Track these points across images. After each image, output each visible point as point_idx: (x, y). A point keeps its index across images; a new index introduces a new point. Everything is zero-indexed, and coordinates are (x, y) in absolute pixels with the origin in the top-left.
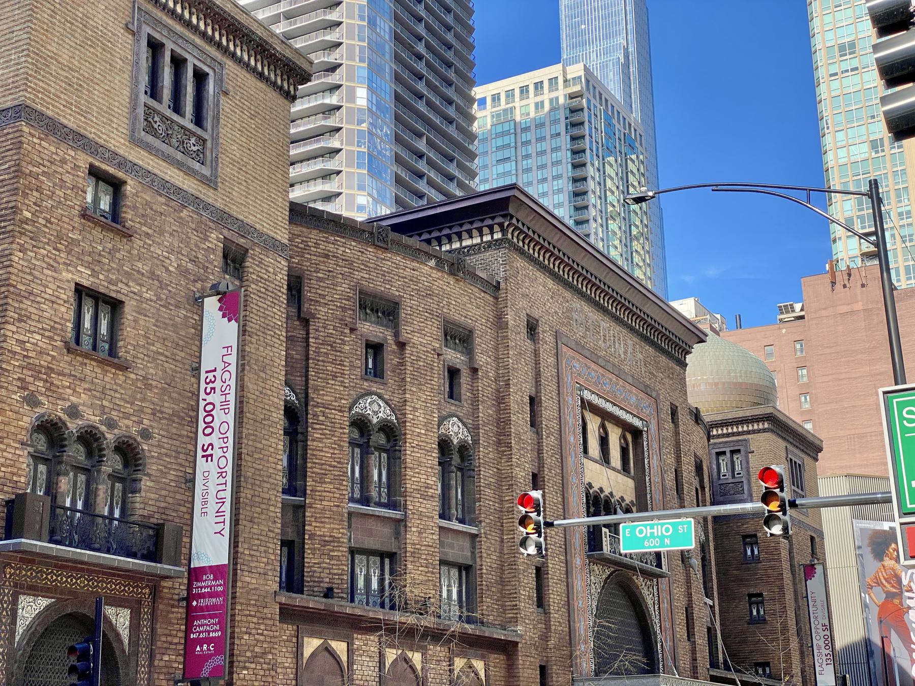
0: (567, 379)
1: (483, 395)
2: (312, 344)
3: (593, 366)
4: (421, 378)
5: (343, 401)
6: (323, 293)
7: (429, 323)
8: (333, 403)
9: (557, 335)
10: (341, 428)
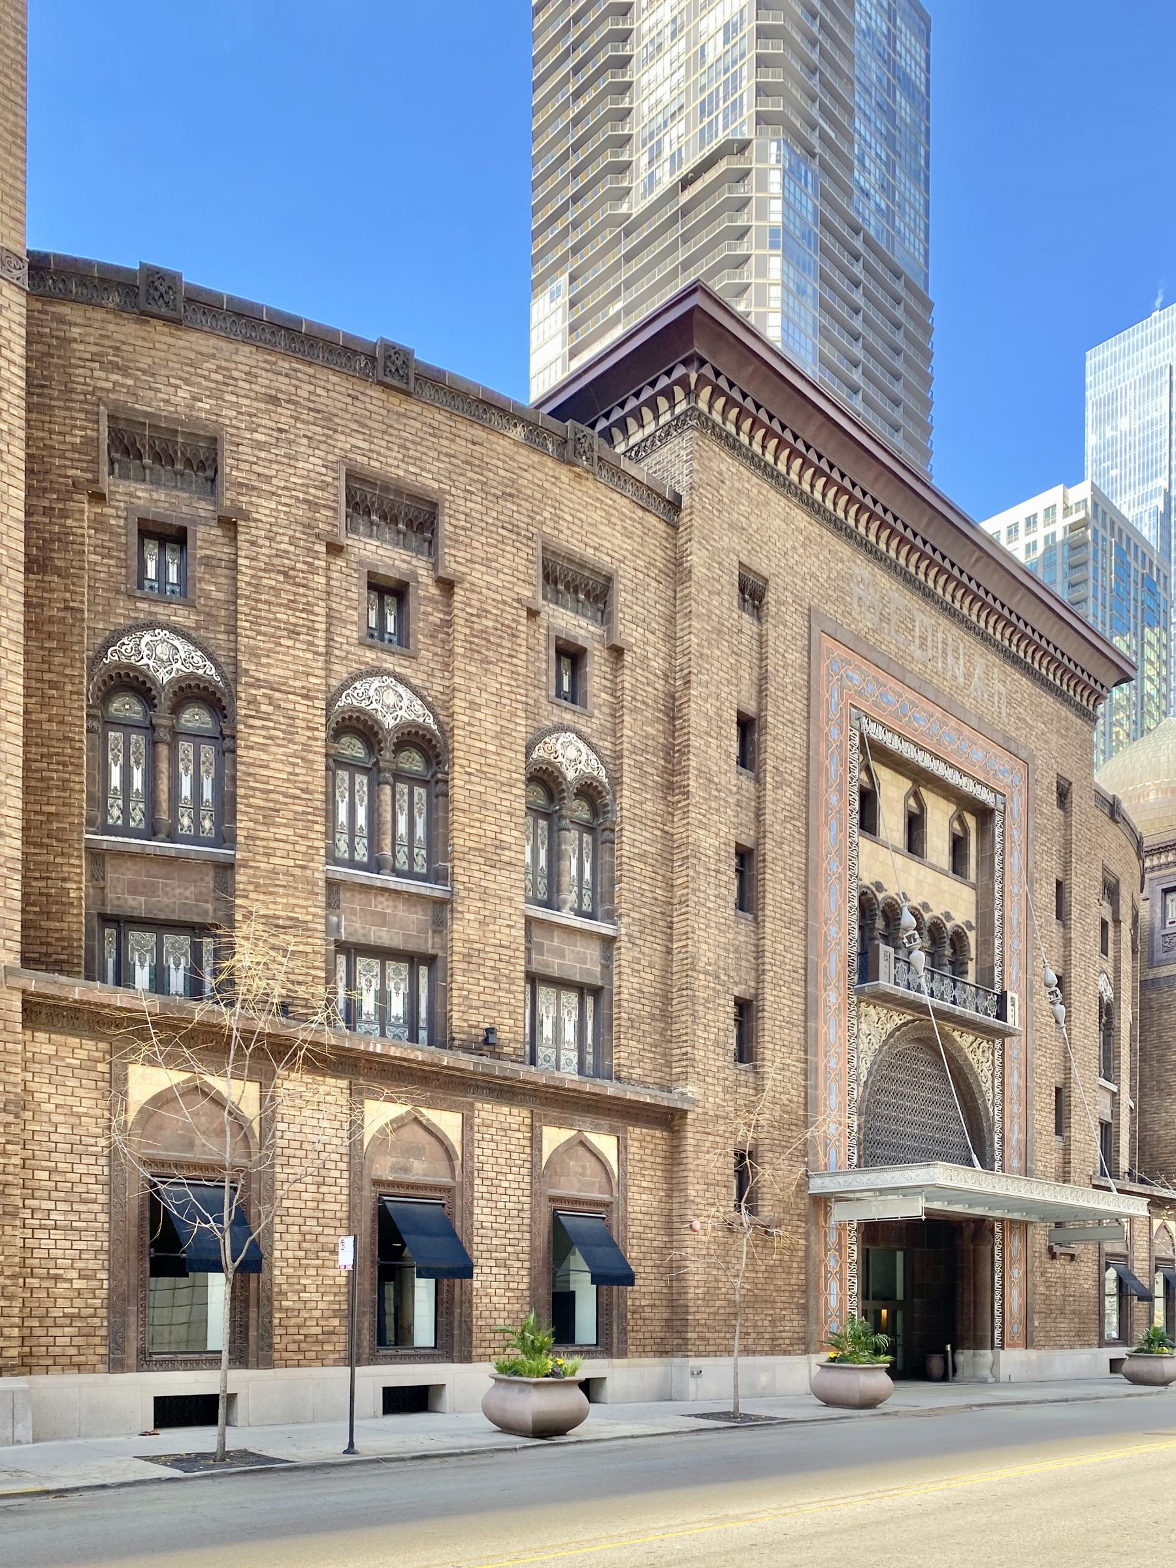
0: (831, 697)
1: (634, 699)
2: (244, 569)
3: (892, 683)
4: (488, 649)
5: (312, 679)
6: (266, 472)
7: (508, 548)
8: (291, 682)
9: (810, 614)
10: (309, 728)
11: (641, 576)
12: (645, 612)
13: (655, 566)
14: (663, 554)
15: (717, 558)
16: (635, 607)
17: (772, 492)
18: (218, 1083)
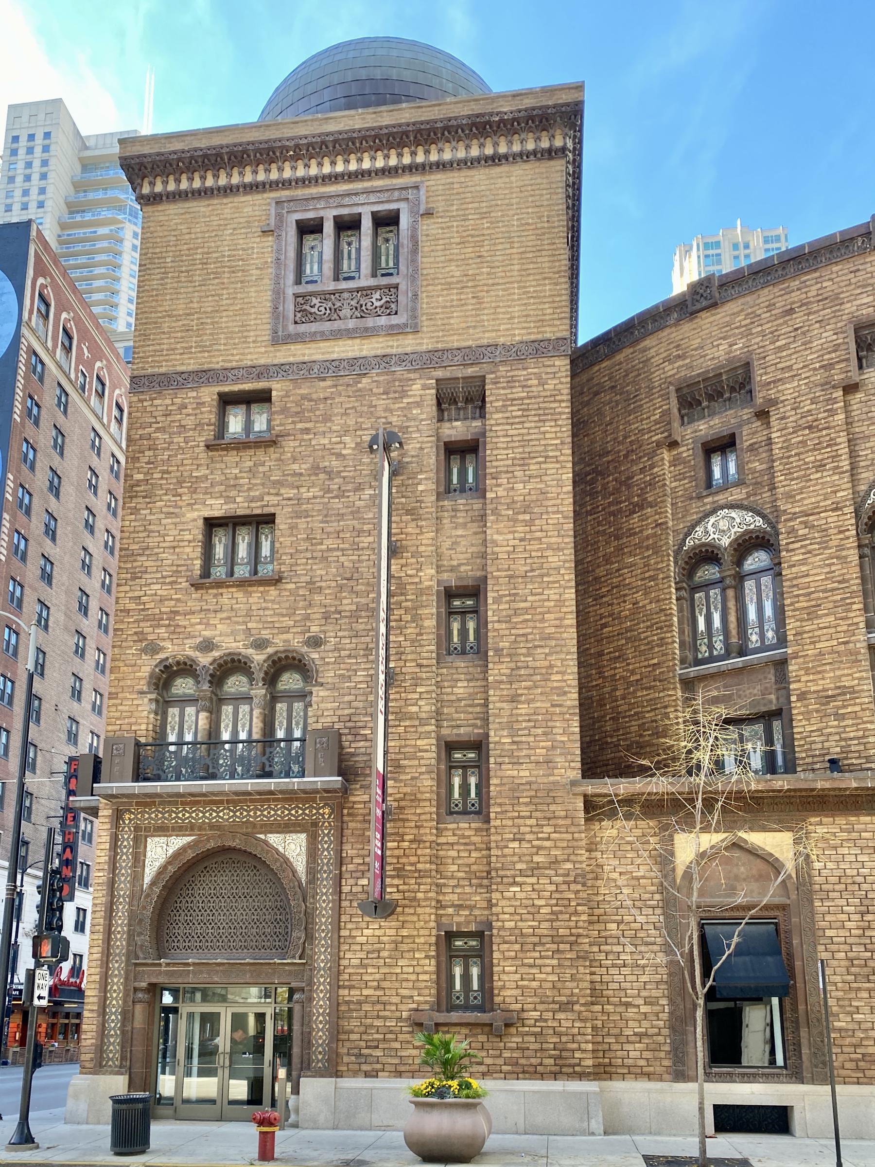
8: (822, 504)
18: (756, 838)
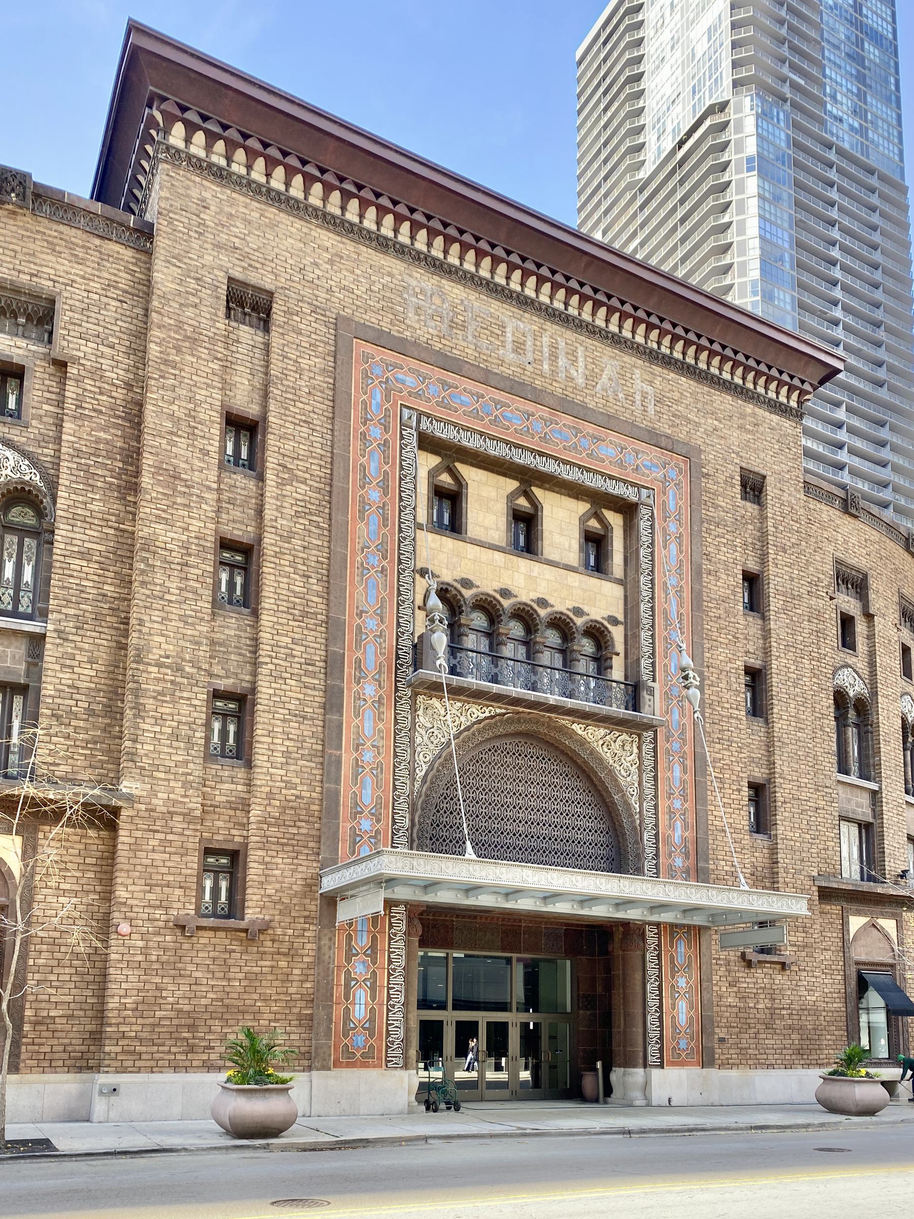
11: (96, 297)
12: (101, 330)
13: (115, 288)
14: (129, 277)
15: (192, 274)
16: (84, 324)
17: (282, 215)
